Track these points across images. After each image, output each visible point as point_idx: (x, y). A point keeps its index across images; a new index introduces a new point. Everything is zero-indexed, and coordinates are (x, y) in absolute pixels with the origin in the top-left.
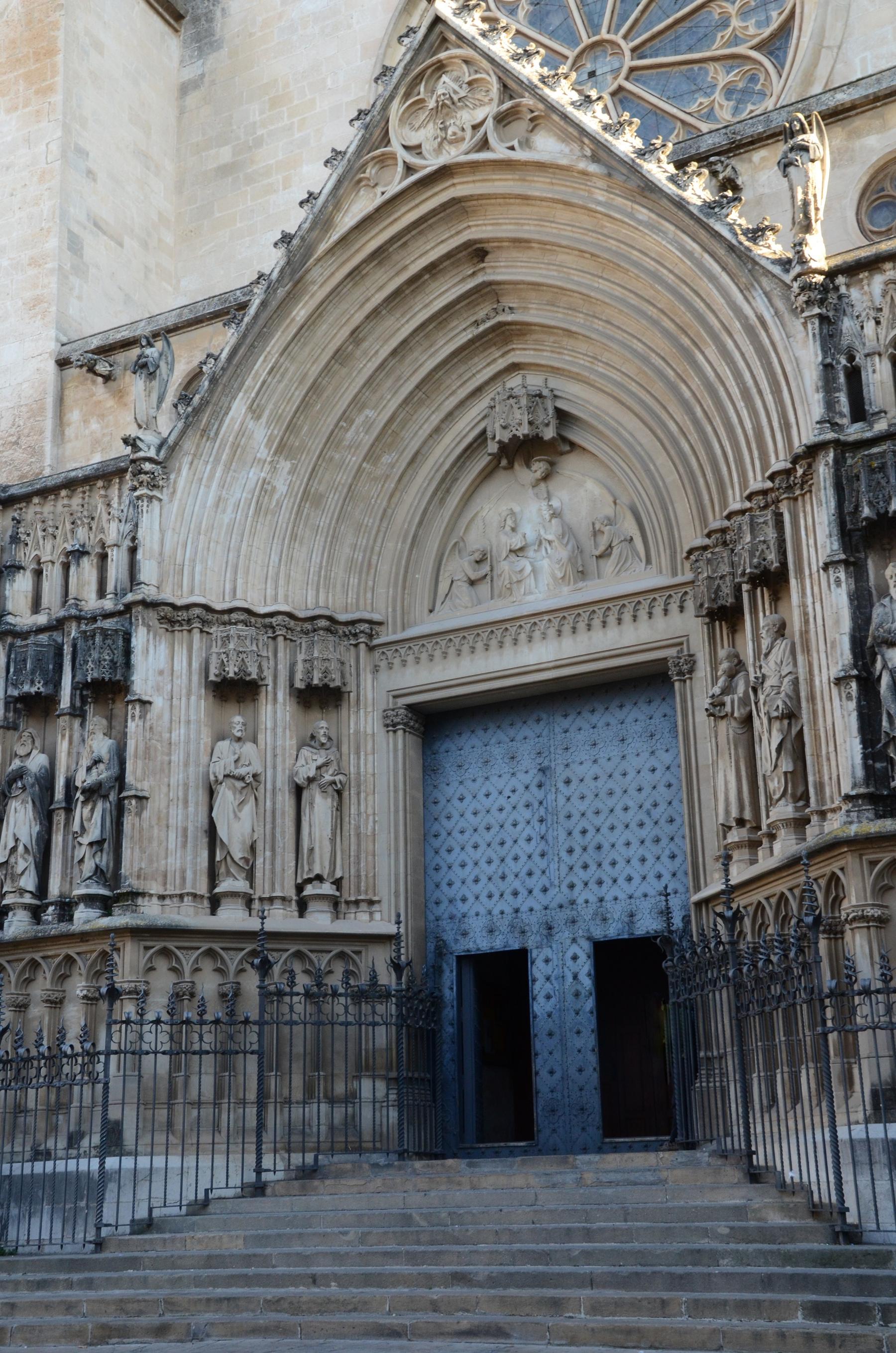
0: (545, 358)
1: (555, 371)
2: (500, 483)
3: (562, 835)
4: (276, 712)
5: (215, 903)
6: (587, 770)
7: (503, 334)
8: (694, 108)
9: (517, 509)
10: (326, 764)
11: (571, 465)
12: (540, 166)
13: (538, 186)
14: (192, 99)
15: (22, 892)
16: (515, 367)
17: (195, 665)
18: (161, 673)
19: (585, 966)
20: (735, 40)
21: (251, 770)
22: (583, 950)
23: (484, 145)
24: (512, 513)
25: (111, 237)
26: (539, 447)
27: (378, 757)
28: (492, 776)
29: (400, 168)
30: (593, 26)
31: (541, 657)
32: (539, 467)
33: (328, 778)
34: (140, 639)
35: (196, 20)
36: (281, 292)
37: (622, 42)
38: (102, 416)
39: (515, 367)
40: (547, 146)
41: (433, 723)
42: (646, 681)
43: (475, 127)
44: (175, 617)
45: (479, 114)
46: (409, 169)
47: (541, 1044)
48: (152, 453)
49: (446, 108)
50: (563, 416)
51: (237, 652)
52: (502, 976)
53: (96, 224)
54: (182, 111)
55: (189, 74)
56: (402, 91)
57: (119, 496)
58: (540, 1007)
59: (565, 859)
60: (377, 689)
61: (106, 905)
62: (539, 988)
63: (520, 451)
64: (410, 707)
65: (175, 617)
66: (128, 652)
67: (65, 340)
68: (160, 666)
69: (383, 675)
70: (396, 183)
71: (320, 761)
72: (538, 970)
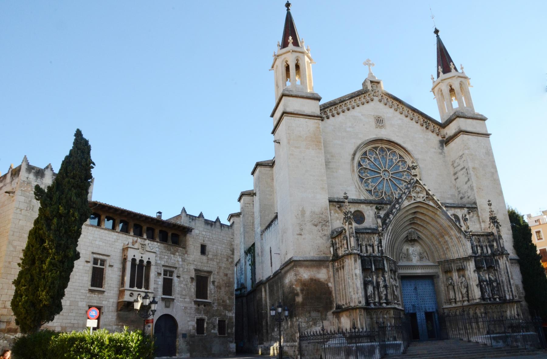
0: (416, 228)
1: (417, 230)
6: (421, 288)
7: (414, 223)
11: (416, 244)
12: (431, 206)
13: (430, 208)
19: (424, 316)
22: (423, 313)
31: (419, 271)
32: (413, 243)
38: (338, 213)
40: (431, 203)
43: (423, 197)
45: (422, 195)
50: (418, 237)
52: (413, 316)
57: (376, 237)
58: (418, 321)
59: (420, 300)
62: (418, 318)
70: (413, 201)
72: (418, 316)
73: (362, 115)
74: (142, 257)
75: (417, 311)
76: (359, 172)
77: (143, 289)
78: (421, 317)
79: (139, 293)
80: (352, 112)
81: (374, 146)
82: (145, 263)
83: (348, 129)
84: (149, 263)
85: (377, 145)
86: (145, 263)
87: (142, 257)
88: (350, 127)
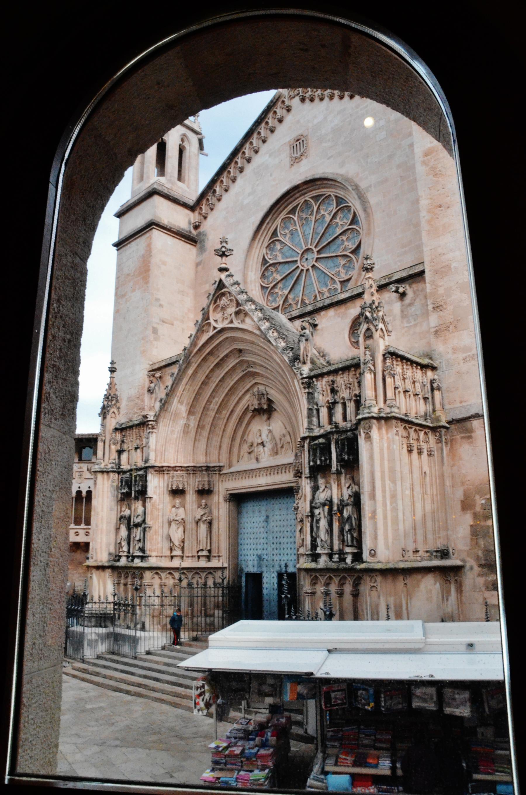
2: (257, 420)
3: (271, 537)
4: (191, 497)
5: (172, 557)
6: (277, 518)
8: (334, 273)
9: (261, 429)
10: (204, 514)
13: (247, 337)
14: (200, 268)
15: (124, 552)
16: (256, 384)
17: (166, 485)
18: (156, 487)
20: (345, 249)
21: (181, 517)
23: (231, 322)
24: (260, 430)
25: (169, 324)
26: (266, 410)
27: (221, 510)
28: (254, 517)
29: (212, 328)
30: (306, 244)
33: (204, 518)
34: (150, 477)
35: (201, 242)
36: (183, 367)
37: (314, 249)
39: (256, 384)
41: (239, 500)
42: (288, 493)
44: (160, 470)
46: (215, 328)
47: (265, 603)
48: (152, 418)
49: (223, 309)
51: (179, 480)
53: (163, 322)
54: (196, 272)
55: (199, 260)
56: (213, 302)
58: (265, 592)
60: (224, 487)
61: (142, 558)
63: (258, 411)
64: (230, 494)
65: (160, 470)
66: (146, 481)
67: (151, 363)
68: (155, 485)
69: (224, 483)
70: (211, 333)
71: (202, 513)
72: (265, 580)
73: (270, 155)
74: (79, 488)
75: (264, 569)
76: (263, 276)
77: (83, 526)
78: (270, 582)
79: (76, 530)
80: (257, 160)
81: (290, 207)
82: (84, 494)
83: (246, 202)
84: (89, 493)
85: (295, 203)
86: (84, 494)
87: (79, 488)
88: (249, 195)
